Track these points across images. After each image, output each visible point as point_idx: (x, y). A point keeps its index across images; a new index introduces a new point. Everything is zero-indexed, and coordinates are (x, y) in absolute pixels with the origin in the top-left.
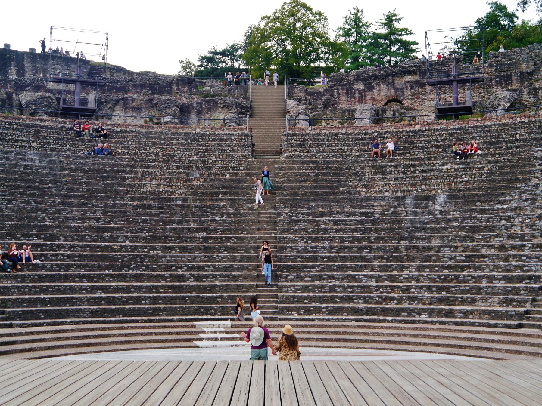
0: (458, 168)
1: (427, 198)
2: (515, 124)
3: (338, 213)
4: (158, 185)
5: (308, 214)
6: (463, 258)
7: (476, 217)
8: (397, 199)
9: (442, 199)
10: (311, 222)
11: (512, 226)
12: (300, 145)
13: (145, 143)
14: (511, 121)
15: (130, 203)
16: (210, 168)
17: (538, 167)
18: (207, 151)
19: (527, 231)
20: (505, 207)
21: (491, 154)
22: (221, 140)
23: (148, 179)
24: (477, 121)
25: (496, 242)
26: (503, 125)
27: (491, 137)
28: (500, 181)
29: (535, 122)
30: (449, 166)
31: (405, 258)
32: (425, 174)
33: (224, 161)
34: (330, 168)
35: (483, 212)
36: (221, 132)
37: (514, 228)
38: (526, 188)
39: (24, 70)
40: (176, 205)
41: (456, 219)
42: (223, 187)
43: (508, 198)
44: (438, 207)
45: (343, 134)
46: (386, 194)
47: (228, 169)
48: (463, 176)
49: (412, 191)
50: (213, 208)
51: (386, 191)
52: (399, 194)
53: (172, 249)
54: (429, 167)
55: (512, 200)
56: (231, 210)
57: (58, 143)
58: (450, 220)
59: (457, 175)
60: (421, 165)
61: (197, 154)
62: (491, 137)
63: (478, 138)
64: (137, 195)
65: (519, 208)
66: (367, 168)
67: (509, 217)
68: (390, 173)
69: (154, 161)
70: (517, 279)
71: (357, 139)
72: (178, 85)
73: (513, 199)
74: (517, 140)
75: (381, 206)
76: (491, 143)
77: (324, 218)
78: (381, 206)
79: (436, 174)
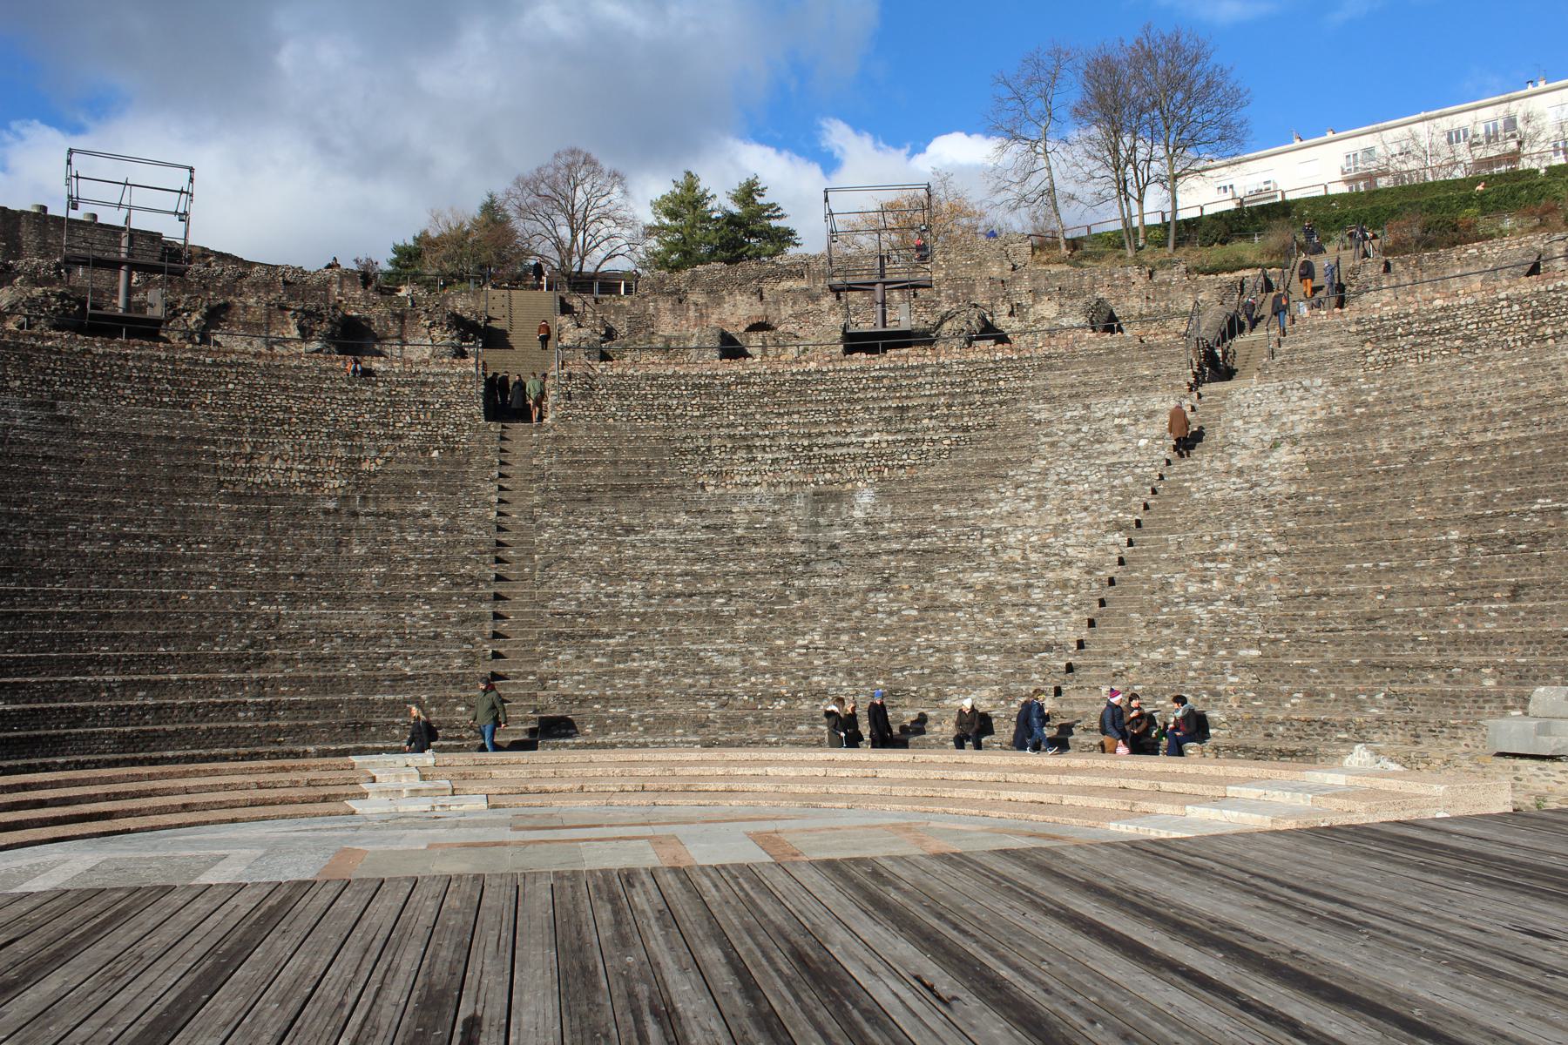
0: (894, 442)
1: (837, 497)
2: (995, 362)
3: (660, 526)
4: (287, 470)
5: (601, 530)
6: (915, 613)
7: (934, 533)
8: (779, 499)
9: (866, 497)
10: (605, 546)
11: (1005, 547)
12: (584, 397)
13: (263, 388)
14: (987, 356)
15: (222, 506)
16: (400, 437)
17: (1044, 439)
18: (393, 404)
19: (1034, 557)
21: (955, 416)
22: (424, 383)
23: (266, 459)
25: (977, 578)
26: (972, 363)
28: (976, 465)
30: (876, 437)
31: (800, 613)
32: (830, 452)
33: (427, 424)
34: (643, 439)
35: (946, 521)
36: (422, 369)
37: (1010, 552)
38: (1025, 478)
39: (19, 247)
40: (327, 512)
41: (897, 537)
42: (424, 474)
43: (993, 496)
44: (858, 514)
45: (668, 377)
46: (756, 489)
47: (436, 441)
49: (807, 483)
50: (404, 515)
51: (757, 484)
52: (782, 490)
53: (313, 600)
54: (839, 439)
55: (1002, 500)
56: (441, 521)
57: (71, 383)
58: (884, 538)
59: (893, 453)
60: (821, 434)
61: (371, 412)
62: (952, 384)
64: (241, 489)
65: (1015, 513)
66: (716, 442)
67: (998, 531)
68: (764, 448)
69: (281, 423)
70: (1023, 650)
71: (695, 386)
72: (341, 287)
74: (1000, 390)
75: (747, 512)
76: (953, 395)
77: (633, 537)
78: (747, 512)
79: (852, 450)
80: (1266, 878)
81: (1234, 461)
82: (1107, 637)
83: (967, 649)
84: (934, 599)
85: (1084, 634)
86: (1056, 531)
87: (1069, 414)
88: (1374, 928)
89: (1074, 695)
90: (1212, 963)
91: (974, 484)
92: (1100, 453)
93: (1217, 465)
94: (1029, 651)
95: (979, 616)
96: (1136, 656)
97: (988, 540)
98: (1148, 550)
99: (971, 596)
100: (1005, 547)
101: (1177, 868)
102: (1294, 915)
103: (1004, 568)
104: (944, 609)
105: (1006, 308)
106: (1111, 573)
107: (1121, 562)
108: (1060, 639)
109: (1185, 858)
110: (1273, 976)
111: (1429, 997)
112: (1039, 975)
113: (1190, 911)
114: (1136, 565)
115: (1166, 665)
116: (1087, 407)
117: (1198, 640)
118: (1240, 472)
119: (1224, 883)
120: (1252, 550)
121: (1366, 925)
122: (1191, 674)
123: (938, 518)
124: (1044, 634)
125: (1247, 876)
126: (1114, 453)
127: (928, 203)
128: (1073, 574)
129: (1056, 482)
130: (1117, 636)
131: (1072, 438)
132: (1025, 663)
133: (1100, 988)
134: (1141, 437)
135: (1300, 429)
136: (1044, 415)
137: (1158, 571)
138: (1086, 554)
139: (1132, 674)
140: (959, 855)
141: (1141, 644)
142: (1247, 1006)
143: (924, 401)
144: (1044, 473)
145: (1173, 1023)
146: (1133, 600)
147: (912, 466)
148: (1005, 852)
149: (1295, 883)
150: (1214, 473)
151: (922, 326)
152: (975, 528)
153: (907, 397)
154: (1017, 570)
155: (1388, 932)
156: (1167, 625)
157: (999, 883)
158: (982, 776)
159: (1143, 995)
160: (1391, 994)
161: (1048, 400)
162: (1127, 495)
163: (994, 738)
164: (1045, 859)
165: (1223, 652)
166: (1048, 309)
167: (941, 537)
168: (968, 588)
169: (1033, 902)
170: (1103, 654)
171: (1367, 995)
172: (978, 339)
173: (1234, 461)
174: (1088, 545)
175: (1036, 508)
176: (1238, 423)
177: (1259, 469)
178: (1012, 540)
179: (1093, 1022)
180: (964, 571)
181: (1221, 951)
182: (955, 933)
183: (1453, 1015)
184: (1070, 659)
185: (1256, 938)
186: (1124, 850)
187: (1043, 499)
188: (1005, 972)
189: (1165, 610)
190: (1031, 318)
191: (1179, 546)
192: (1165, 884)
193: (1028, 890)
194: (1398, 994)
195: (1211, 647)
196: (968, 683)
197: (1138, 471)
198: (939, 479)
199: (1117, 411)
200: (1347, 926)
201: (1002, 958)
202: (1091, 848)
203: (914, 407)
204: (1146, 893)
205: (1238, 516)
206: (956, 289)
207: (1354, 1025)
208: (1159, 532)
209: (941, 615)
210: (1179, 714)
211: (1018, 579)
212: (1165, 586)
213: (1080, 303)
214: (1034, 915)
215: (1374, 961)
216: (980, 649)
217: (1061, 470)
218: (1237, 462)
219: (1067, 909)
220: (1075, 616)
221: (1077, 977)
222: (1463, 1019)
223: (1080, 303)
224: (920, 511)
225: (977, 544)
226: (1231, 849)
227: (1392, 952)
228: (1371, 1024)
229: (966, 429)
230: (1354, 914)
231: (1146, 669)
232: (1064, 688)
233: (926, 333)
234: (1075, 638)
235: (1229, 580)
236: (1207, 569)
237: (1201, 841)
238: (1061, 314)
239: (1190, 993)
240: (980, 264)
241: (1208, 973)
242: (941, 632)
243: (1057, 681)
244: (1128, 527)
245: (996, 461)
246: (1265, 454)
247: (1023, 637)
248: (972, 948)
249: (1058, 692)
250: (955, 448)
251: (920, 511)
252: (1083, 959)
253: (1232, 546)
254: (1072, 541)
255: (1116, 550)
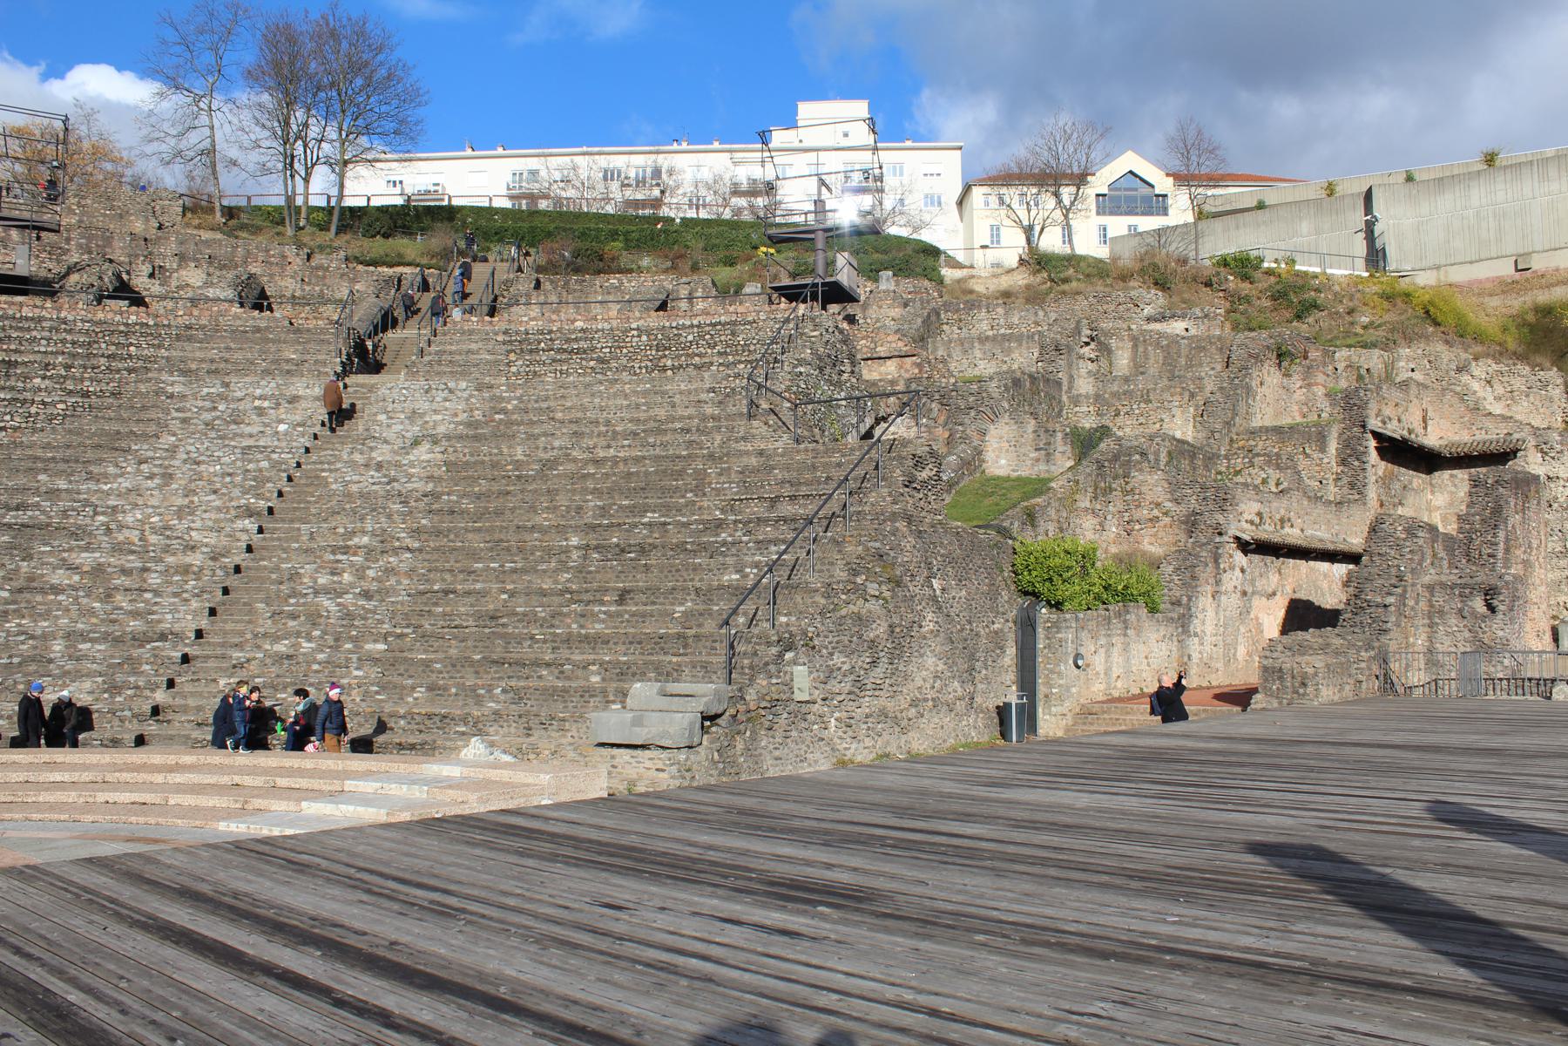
2: (127, 325)
7: (37, 506)
11: (121, 527)
14: (118, 318)
19: (153, 539)
20: (106, 488)
24: (43, 307)
25: (85, 559)
26: (100, 323)
27: (74, 343)
29: (169, 326)
35: (53, 494)
37: (126, 533)
38: (150, 454)
43: (111, 470)
48: (8, 418)
55: (122, 475)
62: (74, 343)
63: (44, 342)
65: (136, 491)
67: (114, 508)
70: (134, 639)
73: (123, 477)
74: (130, 356)
76: (74, 356)
80: (371, 872)
81: (374, 454)
82: (229, 626)
83: (68, 636)
84: (31, 579)
85: (204, 623)
86: (180, 513)
87: (206, 390)
88: (472, 913)
89: (188, 688)
90: (308, 961)
91: (90, 455)
92: (236, 435)
93: (357, 457)
94: (140, 640)
95: (84, 601)
96: (259, 647)
97: (101, 518)
98: (279, 539)
99: (77, 578)
100: (121, 527)
101: (282, 867)
102: (396, 907)
103: (118, 549)
104: (43, 591)
105: (146, 269)
106: (237, 560)
107: (249, 549)
108: (177, 627)
109: (291, 855)
110: (369, 969)
111: (514, 974)
112: (115, 995)
113: (291, 910)
114: (265, 553)
115: (289, 657)
116: (227, 385)
117: (325, 633)
118: (379, 466)
119: (329, 880)
120: (385, 544)
121: (464, 911)
122: (315, 667)
123: (44, 489)
124: (159, 621)
125: (353, 871)
126: (251, 436)
127: (64, 137)
128: (196, 559)
129: (185, 461)
130: (240, 627)
131: (207, 416)
132: (136, 653)
133: (185, 1002)
134: (281, 421)
135: (441, 429)
136: (177, 389)
137: (288, 560)
138: (212, 539)
139: (253, 666)
140: (34, 868)
141: (265, 635)
142: (340, 1003)
143: (38, 357)
144: (173, 450)
145: (261, 1029)
146: (259, 590)
147: (15, 429)
148: (90, 860)
149: (400, 874)
150: (352, 464)
151: (43, 274)
152: (87, 503)
153: (16, 351)
154: (133, 552)
155: (483, 916)
156: (294, 616)
157: (78, 896)
158: (75, 776)
159: (233, 1003)
160: (481, 976)
161: (185, 373)
162: (261, 480)
163: (93, 734)
164: (136, 866)
165: (349, 646)
166: (194, 276)
167: (49, 511)
168: (74, 568)
169: (117, 914)
170: (223, 645)
171: (458, 979)
172: (109, 297)
173: (374, 454)
174: (215, 529)
175: (160, 487)
176: (382, 417)
177: (398, 465)
178: (129, 519)
179: (173, 1040)
180: (70, 550)
181: (319, 948)
182: (16, 958)
183: (534, 989)
184: (187, 650)
185: (356, 932)
186: (227, 851)
187: (168, 477)
188: (74, 996)
189: (292, 601)
190: (174, 283)
191: (312, 536)
192: (268, 884)
193: (113, 901)
194: (488, 975)
195: (337, 640)
196: (66, 673)
197: (275, 456)
198: (47, 446)
199: (258, 392)
200: (445, 913)
201: (74, 982)
202: (190, 851)
203: (25, 363)
204: (246, 895)
205: (374, 510)
206: (90, 238)
207: (444, 1008)
208: (292, 521)
209: (39, 598)
210: (300, 708)
211: (133, 562)
212: (294, 576)
213: (230, 275)
214: (116, 928)
215: (467, 945)
216: (84, 637)
217: (192, 449)
218: (377, 456)
219: (155, 918)
220: (194, 604)
221: (161, 992)
222: (542, 991)
223: (230, 275)
224: (21, 480)
225: (88, 521)
226: (339, 844)
227: (485, 935)
228: (460, 1006)
229: (86, 395)
230: (453, 901)
231: (268, 661)
232: (178, 680)
233: (47, 283)
234: (194, 627)
235: (360, 573)
236: (338, 561)
237: (310, 837)
238: (208, 284)
239: (284, 996)
240: (121, 216)
241: (304, 972)
242: (36, 617)
243: (170, 673)
244: (259, 514)
245: (118, 433)
246: (405, 450)
247: (134, 625)
248: (36, 973)
249: (171, 684)
250: (72, 413)
251: (21, 480)
252: (169, 971)
253: (366, 540)
254: (198, 524)
255: (244, 537)
